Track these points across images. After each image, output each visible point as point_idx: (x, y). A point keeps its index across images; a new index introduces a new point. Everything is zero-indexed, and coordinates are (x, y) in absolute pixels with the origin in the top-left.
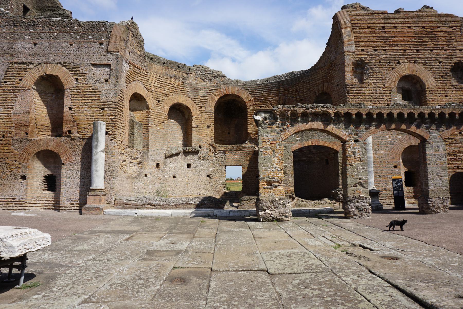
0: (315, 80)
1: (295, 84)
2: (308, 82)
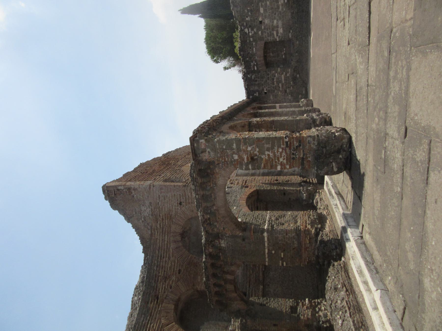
0: (162, 247)
1: (155, 282)
2: (161, 259)
